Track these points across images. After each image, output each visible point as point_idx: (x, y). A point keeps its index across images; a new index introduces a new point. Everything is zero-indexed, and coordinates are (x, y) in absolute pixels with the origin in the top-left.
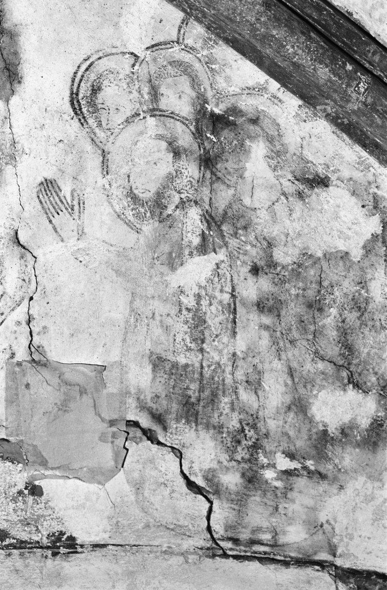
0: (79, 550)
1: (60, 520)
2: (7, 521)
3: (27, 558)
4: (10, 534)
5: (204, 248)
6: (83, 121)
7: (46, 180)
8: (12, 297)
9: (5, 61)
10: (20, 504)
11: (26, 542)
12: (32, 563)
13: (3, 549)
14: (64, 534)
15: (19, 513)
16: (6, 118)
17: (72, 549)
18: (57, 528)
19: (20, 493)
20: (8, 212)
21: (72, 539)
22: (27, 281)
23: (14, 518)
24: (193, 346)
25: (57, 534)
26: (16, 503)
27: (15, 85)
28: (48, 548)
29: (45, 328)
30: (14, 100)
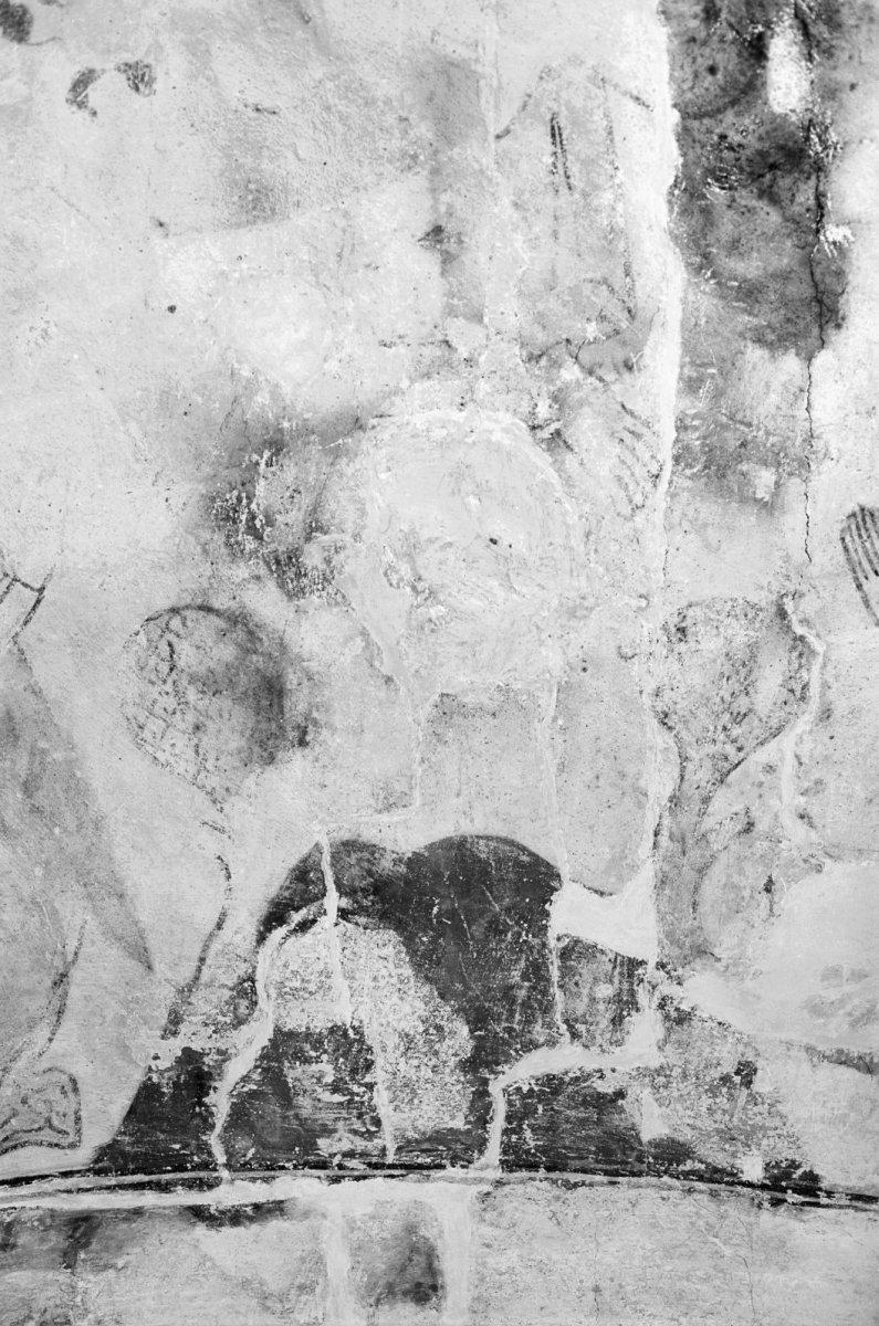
0: (824, 1201)
1: (794, 1140)
2: (693, 1127)
3: (722, 1202)
4: (694, 1153)
7: (863, 510)
8: (765, 719)
9: (816, 286)
10: (722, 1101)
11: (722, 1171)
12: (733, 1213)
13: (678, 1178)
14: (799, 1166)
15: (718, 1116)
16: (802, 390)
17: (811, 1196)
18: (786, 1153)
19: (725, 1079)
20: (780, 563)
21: (812, 1177)
22: (798, 693)
23: (707, 1124)
25: (783, 1165)
26: (715, 1096)
27: (829, 331)
28: (763, 1187)
29: (819, 782)
30: (823, 359)
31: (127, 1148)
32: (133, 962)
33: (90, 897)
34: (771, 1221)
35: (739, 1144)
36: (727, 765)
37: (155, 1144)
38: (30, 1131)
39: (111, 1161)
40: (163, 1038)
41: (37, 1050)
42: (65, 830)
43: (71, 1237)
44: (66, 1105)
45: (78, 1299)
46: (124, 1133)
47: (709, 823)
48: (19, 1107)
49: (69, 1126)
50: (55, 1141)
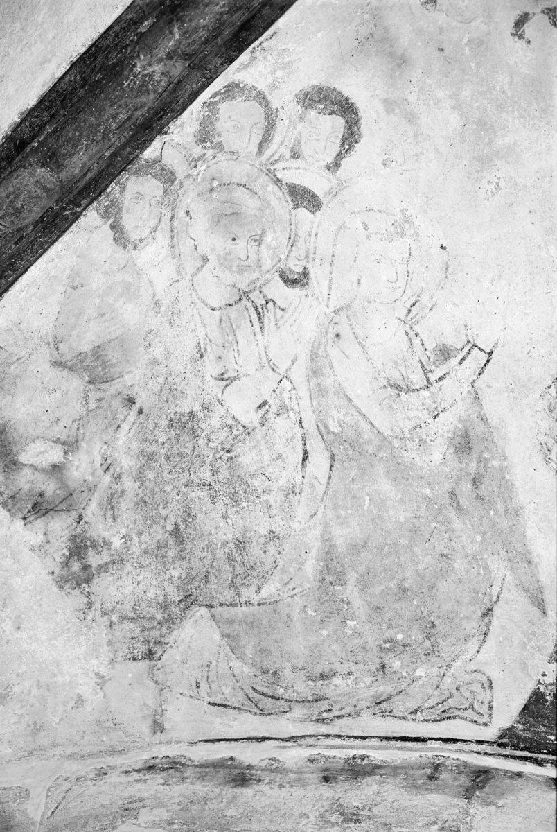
31: (520, 733)
32: (535, 608)
33: (509, 559)
37: (538, 733)
38: (460, 709)
39: (508, 741)
40: (549, 662)
41: (469, 657)
42: (497, 513)
43: (473, 781)
44: (484, 696)
45: (468, 819)
46: (519, 722)
48: (454, 692)
49: (484, 710)
50: (475, 719)
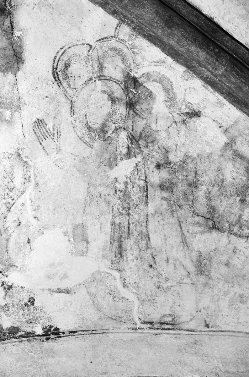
0: (62, 335)
1: (49, 319)
2: (19, 321)
3: (32, 342)
4: (20, 329)
5: (129, 155)
6: (60, 84)
7: (38, 120)
8: (19, 189)
9: (14, 51)
10: (26, 311)
13: (17, 338)
14: (53, 327)
15: (26, 316)
16: (15, 84)
17: (58, 335)
18: (48, 324)
19: (26, 304)
20: (16, 139)
21: (57, 329)
22: (28, 179)
23: (23, 319)
24: (124, 212)
25: (48, 327)
27: (20, 65)
28: (43, 335)
29: (38, 206)
30: (20, 74)
34: (47, 345)
35: (33, 324)
36: (10, 205)
47: (7, 224)
